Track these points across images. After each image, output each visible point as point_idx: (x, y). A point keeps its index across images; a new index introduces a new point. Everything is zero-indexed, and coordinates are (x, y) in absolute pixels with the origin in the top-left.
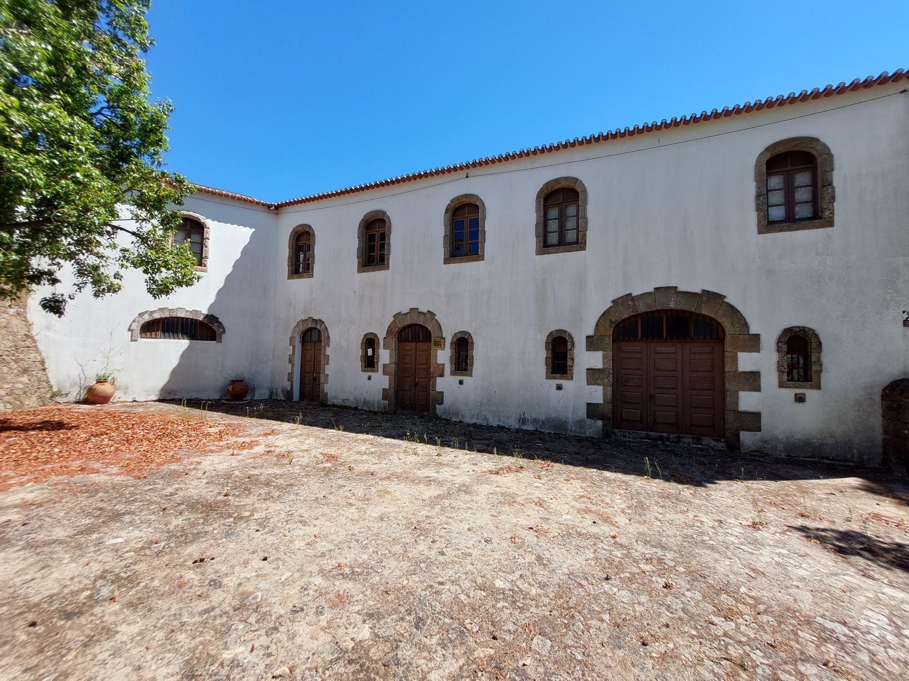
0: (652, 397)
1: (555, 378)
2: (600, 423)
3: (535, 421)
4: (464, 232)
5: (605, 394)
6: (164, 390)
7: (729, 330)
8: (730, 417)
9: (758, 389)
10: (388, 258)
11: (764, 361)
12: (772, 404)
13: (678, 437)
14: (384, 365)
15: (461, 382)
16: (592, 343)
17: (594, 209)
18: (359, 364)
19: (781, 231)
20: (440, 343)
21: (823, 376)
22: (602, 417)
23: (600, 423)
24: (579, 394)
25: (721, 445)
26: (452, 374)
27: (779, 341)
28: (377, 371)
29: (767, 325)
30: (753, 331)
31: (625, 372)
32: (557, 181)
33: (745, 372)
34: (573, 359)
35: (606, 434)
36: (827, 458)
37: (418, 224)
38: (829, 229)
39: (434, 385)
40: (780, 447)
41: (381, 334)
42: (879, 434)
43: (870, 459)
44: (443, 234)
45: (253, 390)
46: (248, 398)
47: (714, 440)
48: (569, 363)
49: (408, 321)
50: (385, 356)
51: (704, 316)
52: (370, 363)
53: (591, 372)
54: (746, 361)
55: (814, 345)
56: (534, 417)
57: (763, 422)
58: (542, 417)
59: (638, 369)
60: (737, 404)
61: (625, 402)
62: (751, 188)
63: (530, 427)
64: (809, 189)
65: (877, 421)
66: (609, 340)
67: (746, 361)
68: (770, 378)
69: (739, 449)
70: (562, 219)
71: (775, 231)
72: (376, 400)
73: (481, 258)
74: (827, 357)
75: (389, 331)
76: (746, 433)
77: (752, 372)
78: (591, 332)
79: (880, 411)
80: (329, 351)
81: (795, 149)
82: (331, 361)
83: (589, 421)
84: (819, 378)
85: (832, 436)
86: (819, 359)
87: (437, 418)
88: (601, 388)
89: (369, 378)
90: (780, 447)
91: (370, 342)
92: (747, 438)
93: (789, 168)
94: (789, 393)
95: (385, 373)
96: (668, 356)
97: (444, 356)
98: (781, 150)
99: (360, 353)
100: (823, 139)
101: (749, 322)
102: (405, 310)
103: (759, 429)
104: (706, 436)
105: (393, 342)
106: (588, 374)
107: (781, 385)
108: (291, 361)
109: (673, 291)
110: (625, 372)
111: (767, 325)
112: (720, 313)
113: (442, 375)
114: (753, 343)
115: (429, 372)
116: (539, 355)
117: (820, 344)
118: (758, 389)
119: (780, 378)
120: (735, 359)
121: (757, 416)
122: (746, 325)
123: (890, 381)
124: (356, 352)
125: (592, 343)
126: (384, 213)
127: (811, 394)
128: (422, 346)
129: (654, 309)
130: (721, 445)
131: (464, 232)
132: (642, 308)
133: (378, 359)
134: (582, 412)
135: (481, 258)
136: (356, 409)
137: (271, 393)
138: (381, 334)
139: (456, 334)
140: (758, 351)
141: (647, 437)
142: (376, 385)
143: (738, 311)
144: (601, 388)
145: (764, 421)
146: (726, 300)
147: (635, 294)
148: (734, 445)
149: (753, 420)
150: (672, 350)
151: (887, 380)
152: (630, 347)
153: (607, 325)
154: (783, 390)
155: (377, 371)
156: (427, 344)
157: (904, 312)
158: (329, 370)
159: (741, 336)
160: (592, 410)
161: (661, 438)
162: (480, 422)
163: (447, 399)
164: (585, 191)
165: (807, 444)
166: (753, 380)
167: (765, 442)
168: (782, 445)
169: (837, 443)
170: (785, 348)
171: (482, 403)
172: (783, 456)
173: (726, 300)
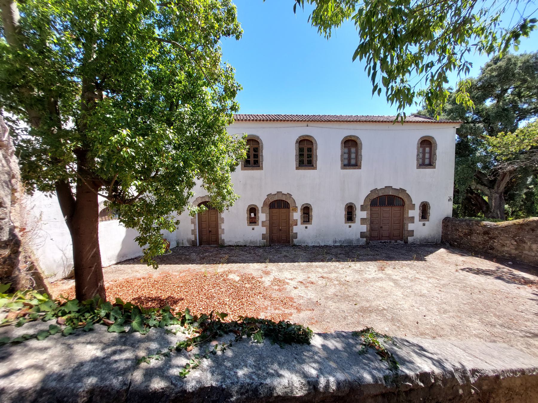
0: (381, 227)
2: (365, 239)
3: (340, 241)
4: (306, 154)
5: (367, 228)
6: (119, 256)
10: (262, 164)
11: (415, 213)
14: (263, 222)
15: (306, 228)
16: (363, 208)
17: (365, 152)
22: (366, 237)
23: (365, 239)
24: (358, 229)
26: (301, 224)
28: (258, 225)
29: (417, 202)
32: (350, 136)
35: (367, 243)
37: (280, 148)
39: (292, 230)
41: (260, 205)
44: (295, 154)
49: (276, 198)
50: (262, 217)
52: (253, 221)
53: (362, 219)
54: (411, 213)
65: (441, 230)
66: (369, 207)
67: (411, 213)
70: (349, 153)
72: (258, 240)
73: (315, 168)
75: (265, 203)
78: (362, 204)
82: (225, 222)
83: (361, 239)
87: (295, 245)
89: (253, 229)
91: (253, 210)
92: (410, 239)
94: (422, 223)
95: (263, 226)
96: (387, 211)
97: (297, 215)
102: (274, 192)
105: (267, 209)
108: (193, 222)
111: (417, 202)
113: (296, 225)
115: (288, 224)
116: (342, 214)
120: (408, 213)
124: (244, 215)
125: (363, 208)
126: (258, 137)
127: (427, 223)
128: (284, 210)
130: (403, 242)
131: (306, 154)
132: (381, 194)
133: (258, 219)
134: (359, 236)
135: (315, 168)
136: (245, 246)
137: (178, 243)
138: (260, 205)
139: (303, 205)
142: (258, 233)
148: (406, 242)
149: (412, 233)
150: (388, 209)
155: (258, 225)
156: (286, 209)
158: (224, 226)
160: (362, 235)
161: (385, 242)
162: (316, 244)
165: (425, 239)
166: (412, 219)
171: (316, 236)
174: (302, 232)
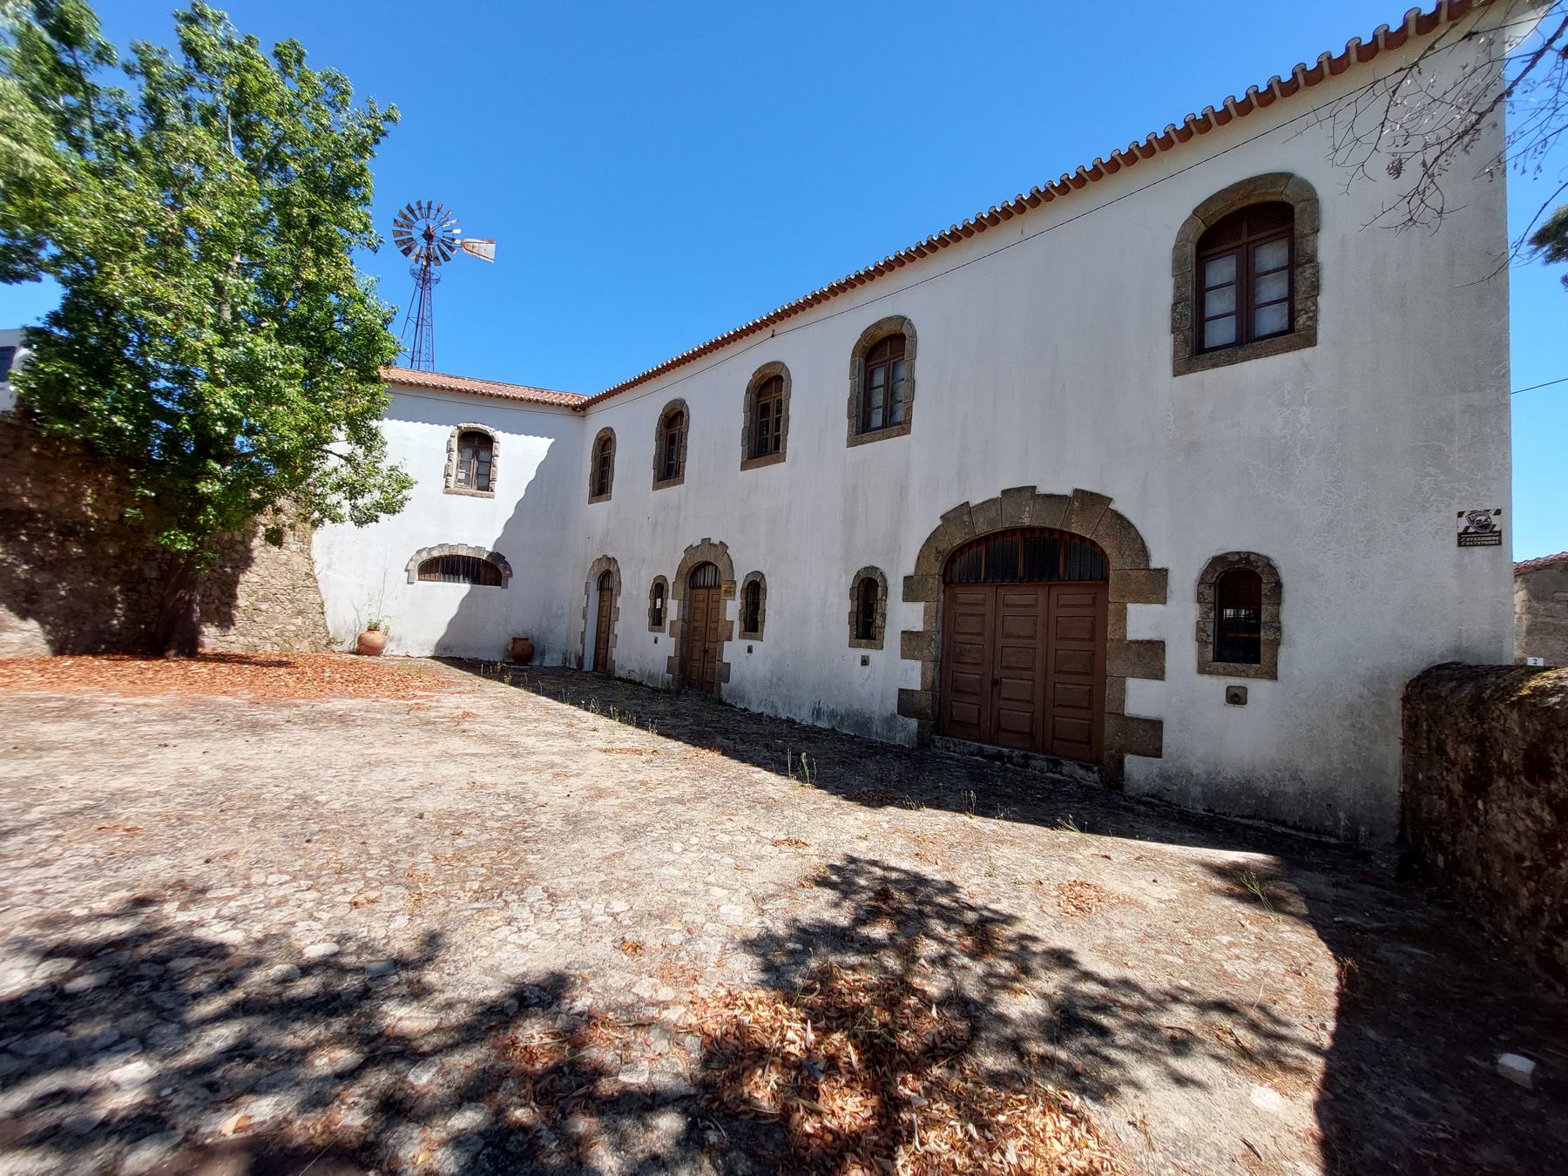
1: (859, 646)
2: (913, 723)
3: (832, 715)
5: (923, 674)
6: (440, 645)
7: (1115, 562)
8: (1110, 725)
9: (1159, 674)
11: (1172, 621)
12: (1187, 709)
13: (1026, 757)
14: (672, 623)
16: (912, 590)
18: (646, 620)
19: (1215, 366)
20: (730, 593)
21: (1283, 652)
22: (917, 714)
23: (913, 723)
24: (889, 675)
25: (1092, 778)
27: (1202, 581)
29: (1182, 553)
30: (1154, 564)
31: (960, 638)
32: (878, 325)
33: (1136, 642)
34: (884, 616)
35: (923, 742)
36: (1284, 824)
38: (1307, 352)
40: (1195, 791)
42: (1394, 782)
43: (1372, 834)
45: (543, 654)
46: (536, 663)
47: (1082, 767)
48: (879, 621)
51: (1073, 535)
54: (1141, 621)
55: (1265, 589)
56: (832, 707)
57: (1166, 739)
58: (841, 710)
59: (980, 634)
60: (1122, 702)
61: (958, 691)
62: (1163, 290)
63: (823, 724)
64: (1209, 284)
65: (1390, 752)
66: (934, 583)
67: (1141, 621)
68: (1183, 653)
69: (1120, 787)
71: (1204, 368)
74: (1291, 615)
76: (1136, 758)
77: (1149, 642)
78: (910, 571)
79: (1400, 732)
80: (620, 602)
81: (1253, 201)
83: (900, 718)
84: (1275, 656)
85: (1295, 777)
86: (1276, 617)
87: (721, 702)
88: (919, 663)
90: (1195, 791)
92: (1137, 768)
93: (1245, 239)
94: (1216, 686)
95: (671, 635)
96: (1023, 610)
98: (1221, 211)
99: (648, 604)
100: (1301, 172)
101: (1150, 544)
103: (1157, 753)
104: (1070, 759)
106: (903, 639)
107: (1203, 669)
109: (1028, 495)
110: (960, 638)
111: (1182, 553)
112: (1101, 530)
113: (730, 639)
114: (1155, 585)
116: (841, 606)
117: (1278, 586)
118: (1159, 674)
119: (1201, 654)
120: (1122, 616)
121: (1156, 726)
122: (1143, 552)
123: (1424, 666)
125: (912, 590)
127: (1258, 688)
129: (998, 528)
130: (1092, 778)
132: (982, 528)
134: (892, 704)
138: (671, 579)
140: (1164, 602)
141: (980, 752)
143: (1131, 526)
144: (919, 663)
145: (1168, 738)
146: (1112, 506)
147: (974, 502)
148: (1114, 778)
149: (1149, 735)
150: (1028, 599)
151: (1414, 662)
152: (971, 595)
153: (932, 558)
154: (1206, 678)
157: (1460, 514)
159: (1134, 574)
160: (906, 701)
161: (999, 756)
163: (734, 674)
164: (914, 335)
165: (1247, 788)
166: (1150, 658)
167: (1168, 779)
168: (1199, 789)
169: (1304, 794)
170: (1210, 594)
172: (1200, 809)
173: (1112, 506)
174: (746, 663)
